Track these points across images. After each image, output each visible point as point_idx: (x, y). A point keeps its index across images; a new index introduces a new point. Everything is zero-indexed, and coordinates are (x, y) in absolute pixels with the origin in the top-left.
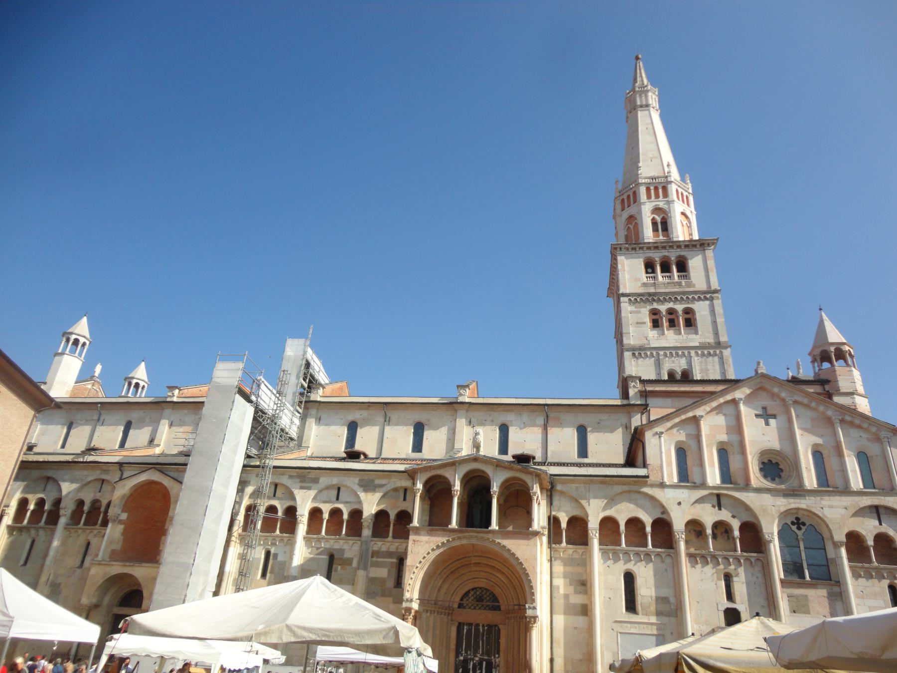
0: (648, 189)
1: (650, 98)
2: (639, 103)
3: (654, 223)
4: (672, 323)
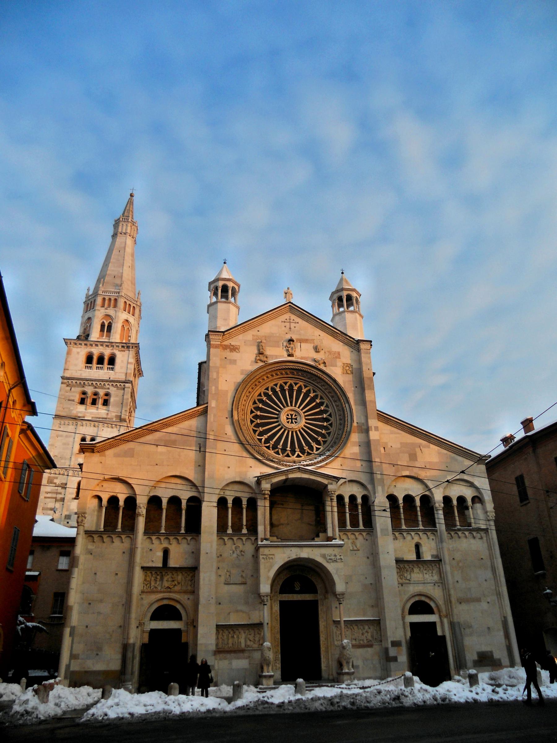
0: (104, 299)
1: (129, 228)
2: (120, 230)
3: (103, 325)
4: (94, 402)
